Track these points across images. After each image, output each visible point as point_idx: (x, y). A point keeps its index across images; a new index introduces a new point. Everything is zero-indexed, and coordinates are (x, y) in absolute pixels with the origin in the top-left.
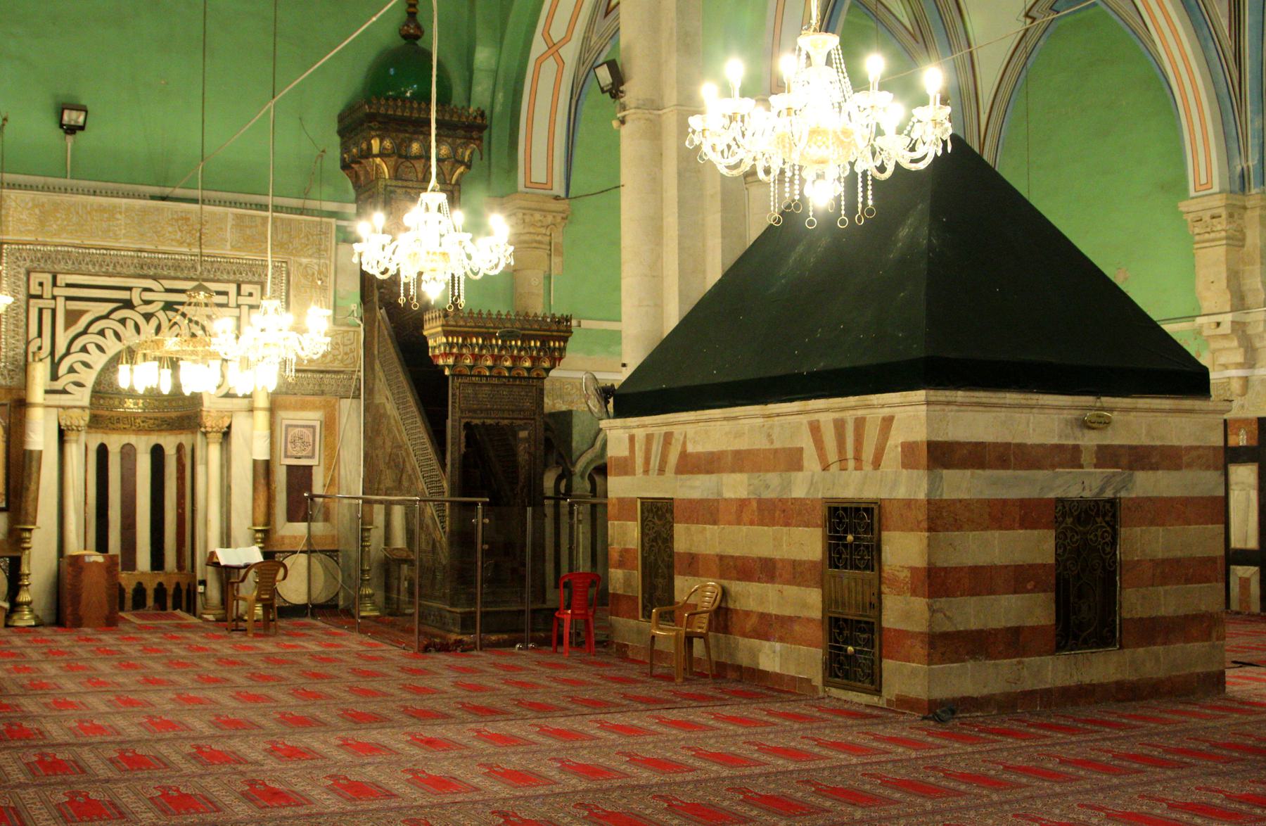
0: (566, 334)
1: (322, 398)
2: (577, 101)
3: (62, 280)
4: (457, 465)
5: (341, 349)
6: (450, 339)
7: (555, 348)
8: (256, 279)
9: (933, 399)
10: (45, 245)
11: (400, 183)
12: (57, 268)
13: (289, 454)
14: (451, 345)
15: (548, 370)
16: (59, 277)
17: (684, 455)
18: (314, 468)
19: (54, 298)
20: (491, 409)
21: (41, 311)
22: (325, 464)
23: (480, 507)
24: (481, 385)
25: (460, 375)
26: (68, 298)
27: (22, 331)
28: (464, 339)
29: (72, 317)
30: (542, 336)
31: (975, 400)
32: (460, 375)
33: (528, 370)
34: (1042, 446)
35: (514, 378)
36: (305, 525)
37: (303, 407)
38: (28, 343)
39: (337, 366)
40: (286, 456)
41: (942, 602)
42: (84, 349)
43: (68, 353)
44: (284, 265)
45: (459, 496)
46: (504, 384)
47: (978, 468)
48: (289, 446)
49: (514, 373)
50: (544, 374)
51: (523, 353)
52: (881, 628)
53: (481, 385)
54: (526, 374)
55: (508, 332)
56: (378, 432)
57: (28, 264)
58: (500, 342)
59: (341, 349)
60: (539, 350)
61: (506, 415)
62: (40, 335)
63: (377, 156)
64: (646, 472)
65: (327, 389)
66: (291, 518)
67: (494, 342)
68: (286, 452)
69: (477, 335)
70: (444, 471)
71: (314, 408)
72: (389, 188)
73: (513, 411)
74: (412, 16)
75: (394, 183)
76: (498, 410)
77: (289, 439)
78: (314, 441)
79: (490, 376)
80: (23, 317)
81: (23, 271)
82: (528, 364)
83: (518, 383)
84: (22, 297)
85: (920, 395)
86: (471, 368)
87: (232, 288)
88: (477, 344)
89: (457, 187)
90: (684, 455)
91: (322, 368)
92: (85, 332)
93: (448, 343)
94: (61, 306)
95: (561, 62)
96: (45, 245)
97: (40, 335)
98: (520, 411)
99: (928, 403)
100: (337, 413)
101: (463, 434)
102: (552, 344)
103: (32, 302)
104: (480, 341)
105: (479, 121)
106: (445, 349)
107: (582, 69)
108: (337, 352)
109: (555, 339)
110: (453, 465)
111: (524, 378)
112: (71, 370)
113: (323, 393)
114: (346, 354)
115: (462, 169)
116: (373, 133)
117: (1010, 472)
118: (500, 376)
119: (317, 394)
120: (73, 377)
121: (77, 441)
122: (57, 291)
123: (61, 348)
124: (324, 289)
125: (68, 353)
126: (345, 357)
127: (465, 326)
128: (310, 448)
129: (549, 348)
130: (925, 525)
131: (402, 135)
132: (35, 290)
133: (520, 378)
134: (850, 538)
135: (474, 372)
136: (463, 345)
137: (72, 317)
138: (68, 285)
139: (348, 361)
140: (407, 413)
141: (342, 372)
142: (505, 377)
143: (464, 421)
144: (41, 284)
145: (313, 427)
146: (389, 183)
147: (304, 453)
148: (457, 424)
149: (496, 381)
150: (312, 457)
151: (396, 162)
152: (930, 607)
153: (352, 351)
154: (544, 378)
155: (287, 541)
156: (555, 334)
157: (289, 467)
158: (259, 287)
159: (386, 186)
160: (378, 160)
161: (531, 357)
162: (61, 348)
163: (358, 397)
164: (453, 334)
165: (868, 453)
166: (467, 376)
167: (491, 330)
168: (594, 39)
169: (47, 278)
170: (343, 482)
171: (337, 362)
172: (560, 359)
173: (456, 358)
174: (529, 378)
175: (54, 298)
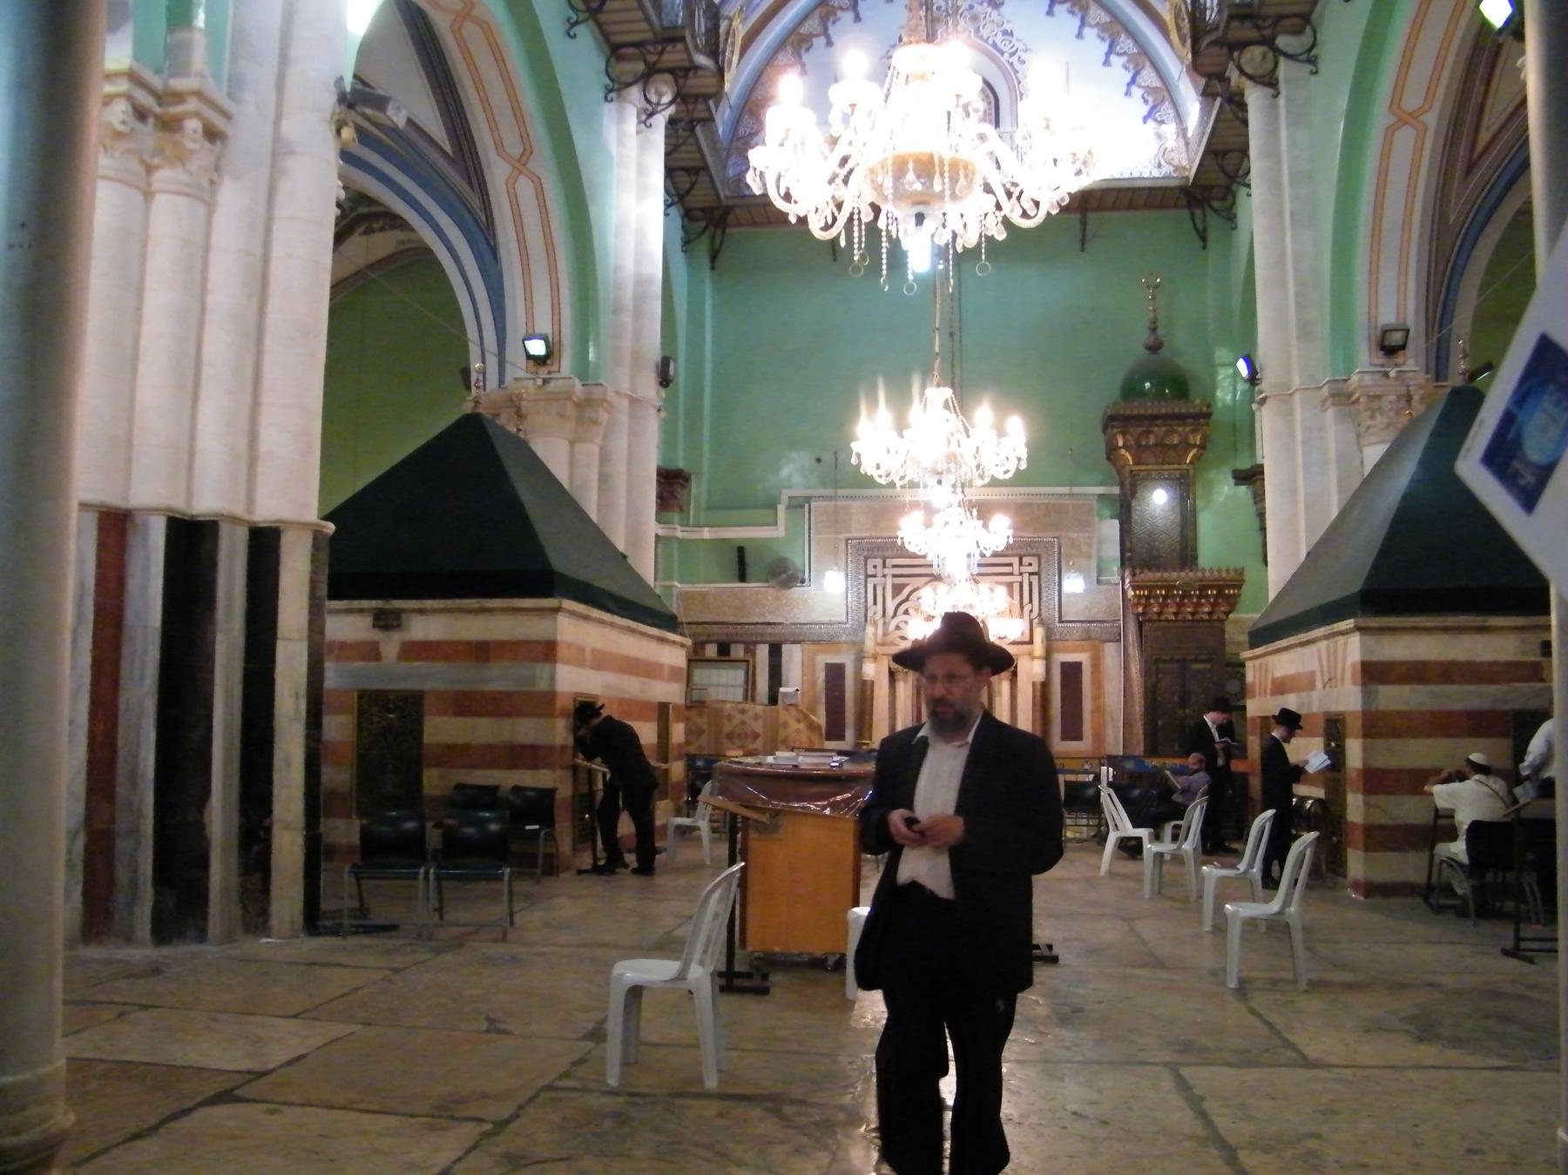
3: (889, 562)
7: (1229, 596)
8: (1034, 551)
9: (1363, 625)
10: (877, 538)
11: (1143, 467)
12: (887, 554)
14: (1139, 597)
15: (1227, 614)
16: (888, 560)
17: (1274, 680)
19: (884, 576)
21: (875, 587)
25: (1151, 621)
26: (894, 576)
27: (863, 600)
29: (897, 589)
30: (1217, 586)
31: (1410, 624)
32: (1151, 621)
33: (1210, 614)
34: (1495, 663)
35: (1198, 621)
38: (866, 610)
39: (1101, 617)
41: (1374, 799)
42: (906, 612)
43: (895, 615)
47: (1418, 684)
49: (1197, 617)
50: (1223, 617)
51: (1203, 601)
52: (1346, 821)
57: (866, 553)
60: (1216, 597)
62: (875, 603)
63: (1121, 448)
64: (1260, 694)
65: (1093, 635)
66: (1066, 736)
69: (1161, 588)
74: (1154, 330)
75: (1138, 468)
79: (1176, 621)
80: (862, 591)
81: (862, 558)
82: (1207, 609)
84: (862, 577)
85: (1348, 624)
86: (1160, 614)
87: (1015, 561)
88: (1161, 594)
89: (1191, 466)
90: (1274, 680)
92: (906, 600)
93: (1135, 596)
94: (889, 581)
96: (877, 538)
97: (875, 603)
99: (1358, 629)
103: (869, 579)
104: (1163, 592)
105: (1205, 410)
109: (1229, 587)
112: (898, 628)
113: (1089, 638)
115: (1194, 451)
116: (1115, 430)
117: (1455, 687)
118: (1185, 620)
120: (899, 633)
121: (905, 680)
122: (886, 571)
123: (890, 611)
124: (1089, 556)
125: (895, 615)
129: (1225, 595)
130: (1360, 733)
131: (1140, 430)
132: (871, 571)
133: (1202, 620)
134: (1333, 744)
135: (1163, 618)
136: (1148, 598)
137: (897, 589)
138: (894, 566)
143: (1154, 657)
144: (875, 567)
146: (1133, 468)
149: (1181, 624)
152: (1366, 803)
154: (1224, 620)
158: (1036, 559)
159: (1131, 471)
160: (1123, 451)
161: (1210, 603)
162: (890, 611)
163: (1119, 640)
164: (1140, 588)
165: (1339, 677)
166: (1155, 621)
169: (879, 562)
175: (884, 576)
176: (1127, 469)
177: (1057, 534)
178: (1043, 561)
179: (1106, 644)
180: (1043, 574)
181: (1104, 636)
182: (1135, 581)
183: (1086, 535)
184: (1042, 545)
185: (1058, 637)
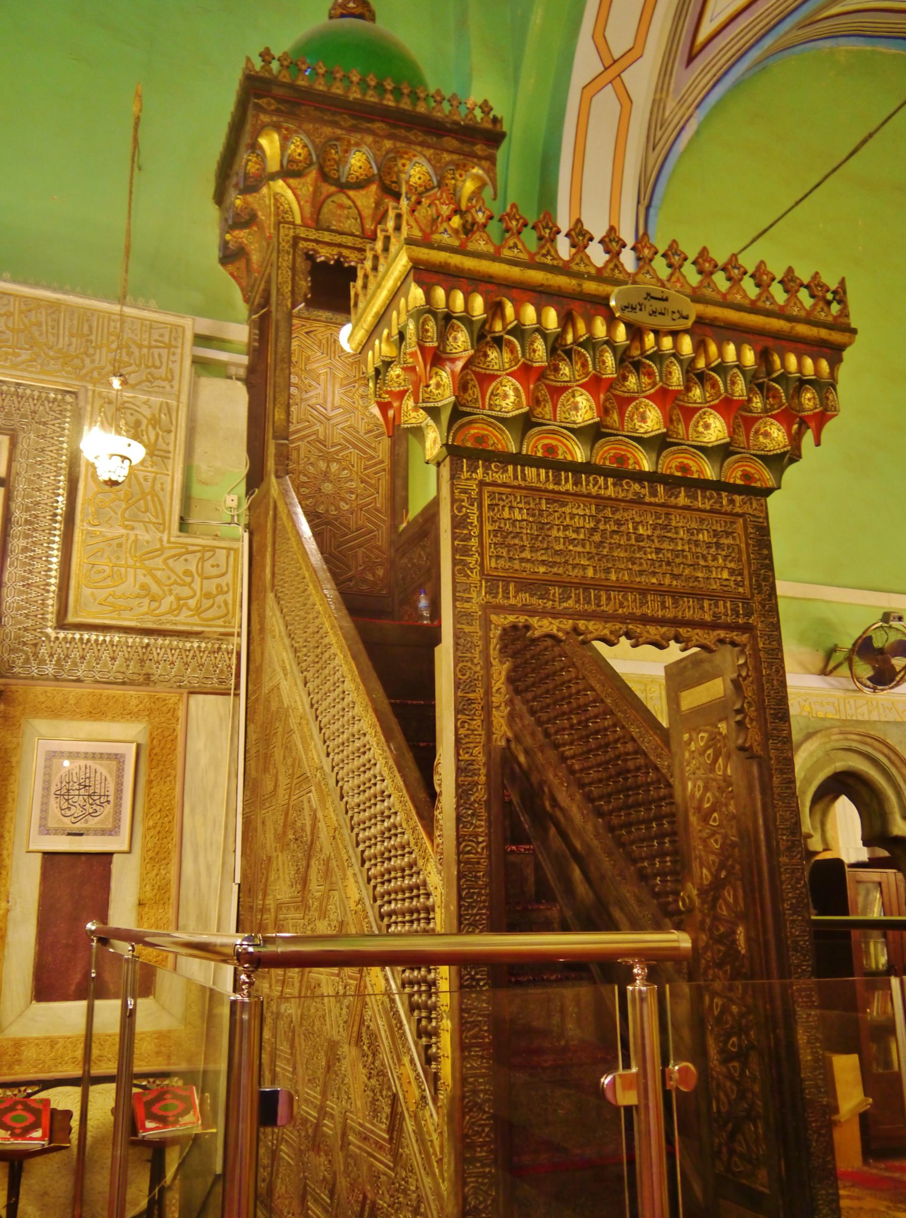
0: (836, 337)
1: (142, 693)
2: (648, 208)
4: (480, 794)
5: (197, 586)
6: (440, 293)
7: (803, 383)
11: (327, 237)
13: (51, 824)
14: (447, 320)
18: (117, 862)
20: (597, 586)
22: (145, 850)
23: (639, 986)
24: (557, 498)
28: (495, 309)
35: (672, 483)
36: (84, 1004)
37: (96, 712)
39: (184, 621)
40: (45, 830)
44: (68, 398)
45: (495, 927)
46: (638, 501)
48: (53, 803)
49: (670, 464)
50: (767, 477)
53: (557, 498)
54: (710, 473)
55: (649, 296)
56: (266, 760)
58: (621, 333)
59: (197, 586)
61: (652, 608)
65: (157, 671)
67: (600, 328)
68: (44, 818)
70: (429, 822)
71: (126, 714)
72: (302, 245)
73: (677, 595)
75: (313, 234)
76: (624, 588)
77: (53, 789)
78: (119, 791)
79: (588, 468)
83: (682, 500)
91: (149, 625)
93: (429, 309)
95: (626, 99)
98: (698, 596)
100: (180, 728)
101: (500, 670)
102: (792, 360)
106: (422, 331)
107: (652, 157)
108: (186, 592)
110: (463, 792)
111: (704, 485)
114: (208, 596)
119: (132, 683)
126: (207, 603)
127: (495, 257)
128: (109, 808)
135: (534, 446)
139: (209, 614)
140: (325, 680)
141: (197, 634)
142: (640, 477)
145: (118, 758)
146: (302, 232)
147: (93, 823)
148: (475, 629)
150: (113, 831)
151: (316, 191)
153: (221, 591)
154: (768, 491)
155: (30, 1053)
156: (802, 329)
157: (48, 856)
159: (296, 239)
167: (591, 287)
168: (671, 104)
170: (188, 892)
171: (185, 613)
172: (822, 418)
173: (462, 386)
174: (719, 486)
176: (287, 233)
177: (75, 384)
178: (23, 445)
179: (197, 701)
180: (21, 486)
181: (193, 677)
182: (426, 242)
183: (156, 400)
184: (28, 407)
185: (50, 669)
